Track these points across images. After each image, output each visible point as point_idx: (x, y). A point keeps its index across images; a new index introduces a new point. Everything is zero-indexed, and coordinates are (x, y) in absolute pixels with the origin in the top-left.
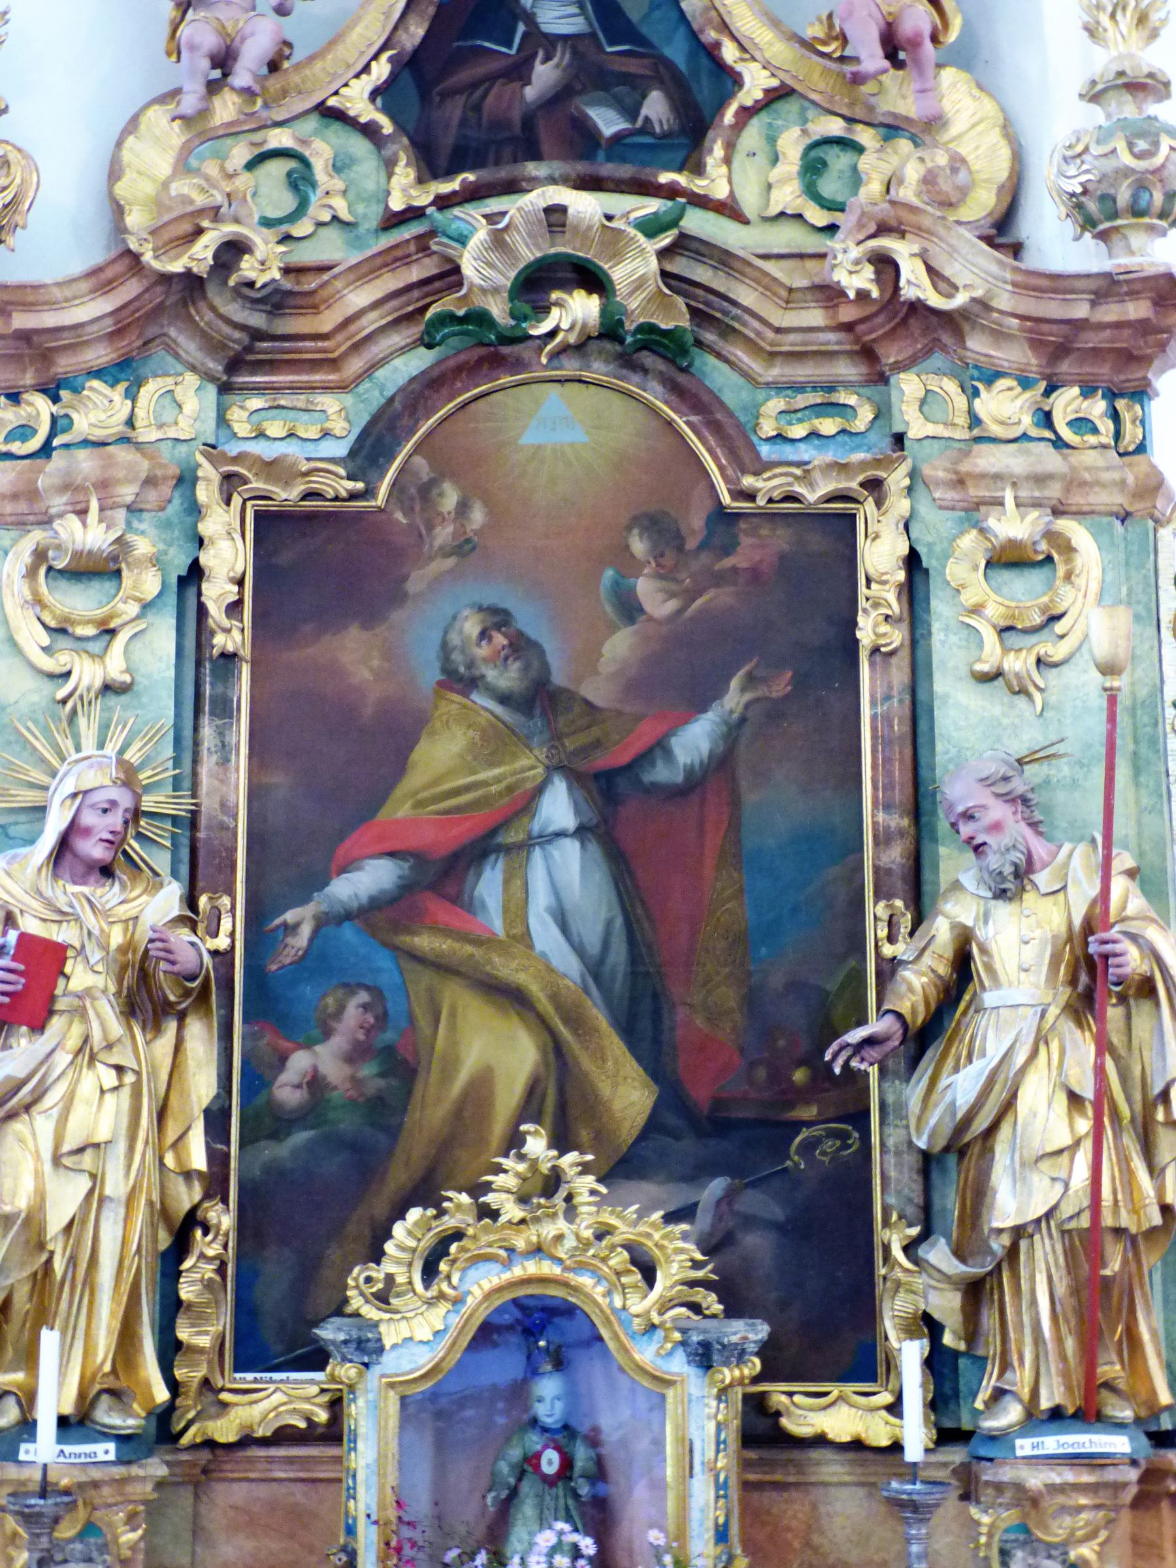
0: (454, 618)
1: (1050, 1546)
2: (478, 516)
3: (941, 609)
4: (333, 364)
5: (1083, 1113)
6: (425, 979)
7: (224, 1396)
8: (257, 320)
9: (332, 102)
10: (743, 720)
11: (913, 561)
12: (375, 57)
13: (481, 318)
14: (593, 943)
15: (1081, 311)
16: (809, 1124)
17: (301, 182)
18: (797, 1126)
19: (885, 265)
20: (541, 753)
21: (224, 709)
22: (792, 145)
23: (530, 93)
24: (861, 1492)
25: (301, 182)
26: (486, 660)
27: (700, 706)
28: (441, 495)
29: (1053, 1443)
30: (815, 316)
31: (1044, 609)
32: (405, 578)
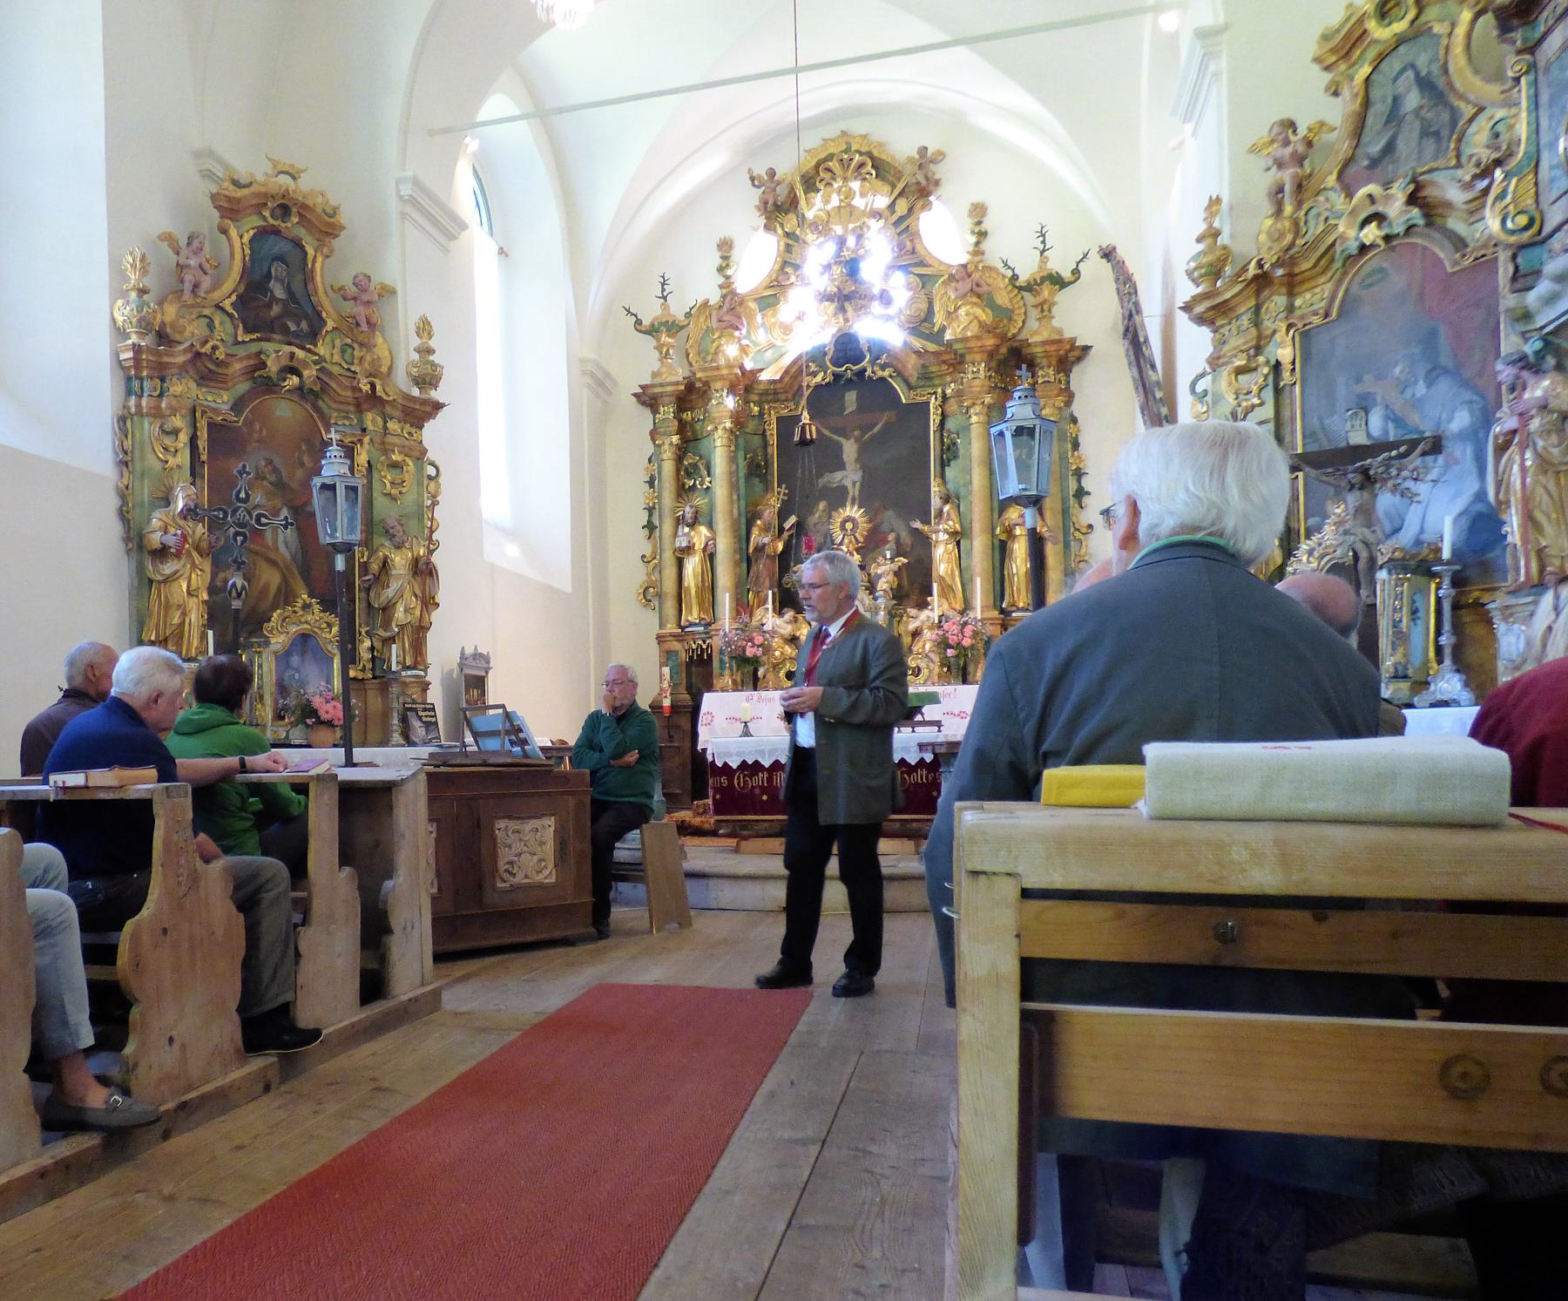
3: (375, 475)
22: (338, 342)
25: (211, 326)
30: (349, 394)
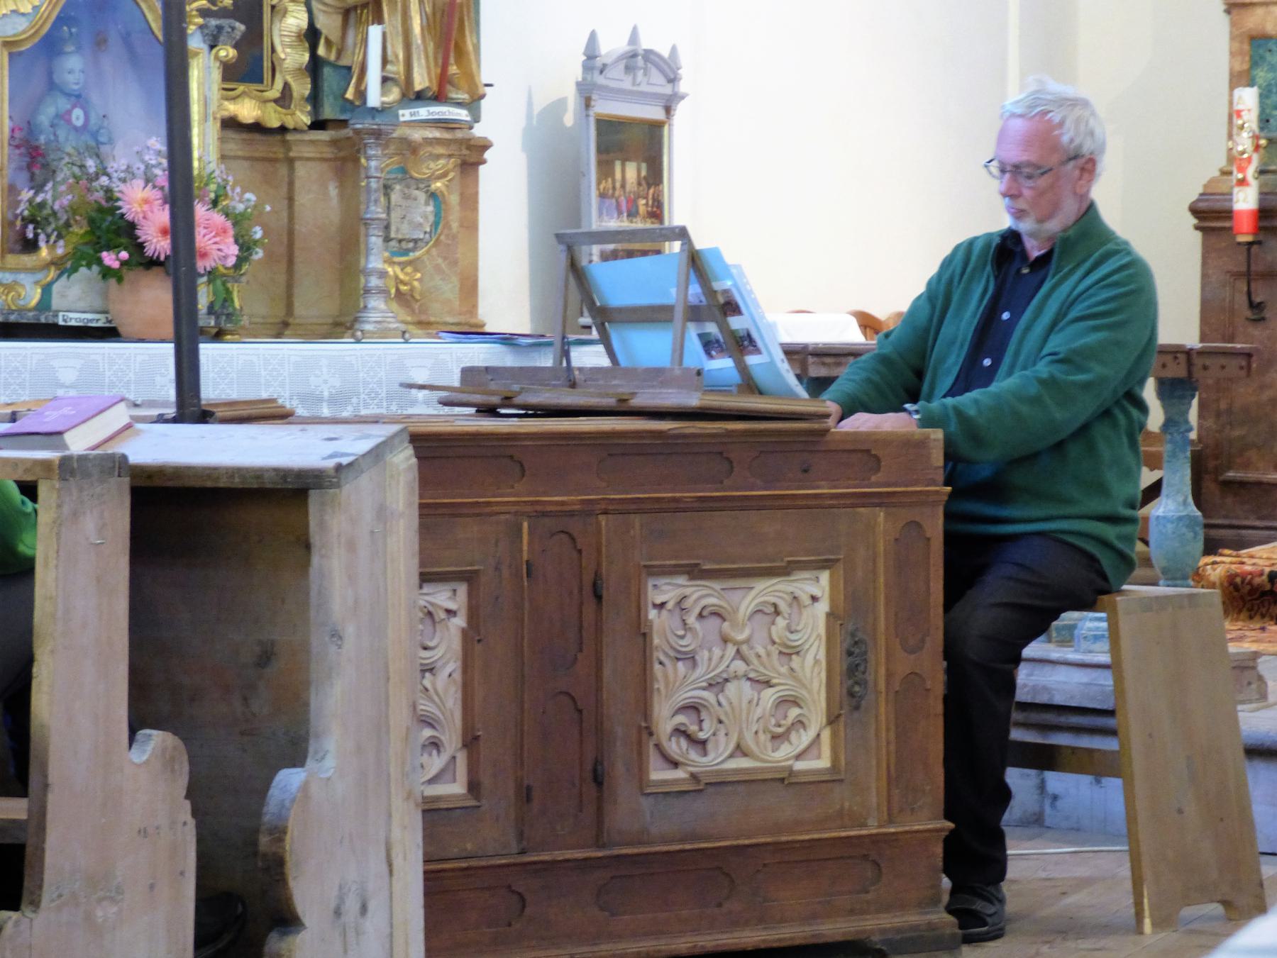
1: (421, 181)
29: (424, 112)
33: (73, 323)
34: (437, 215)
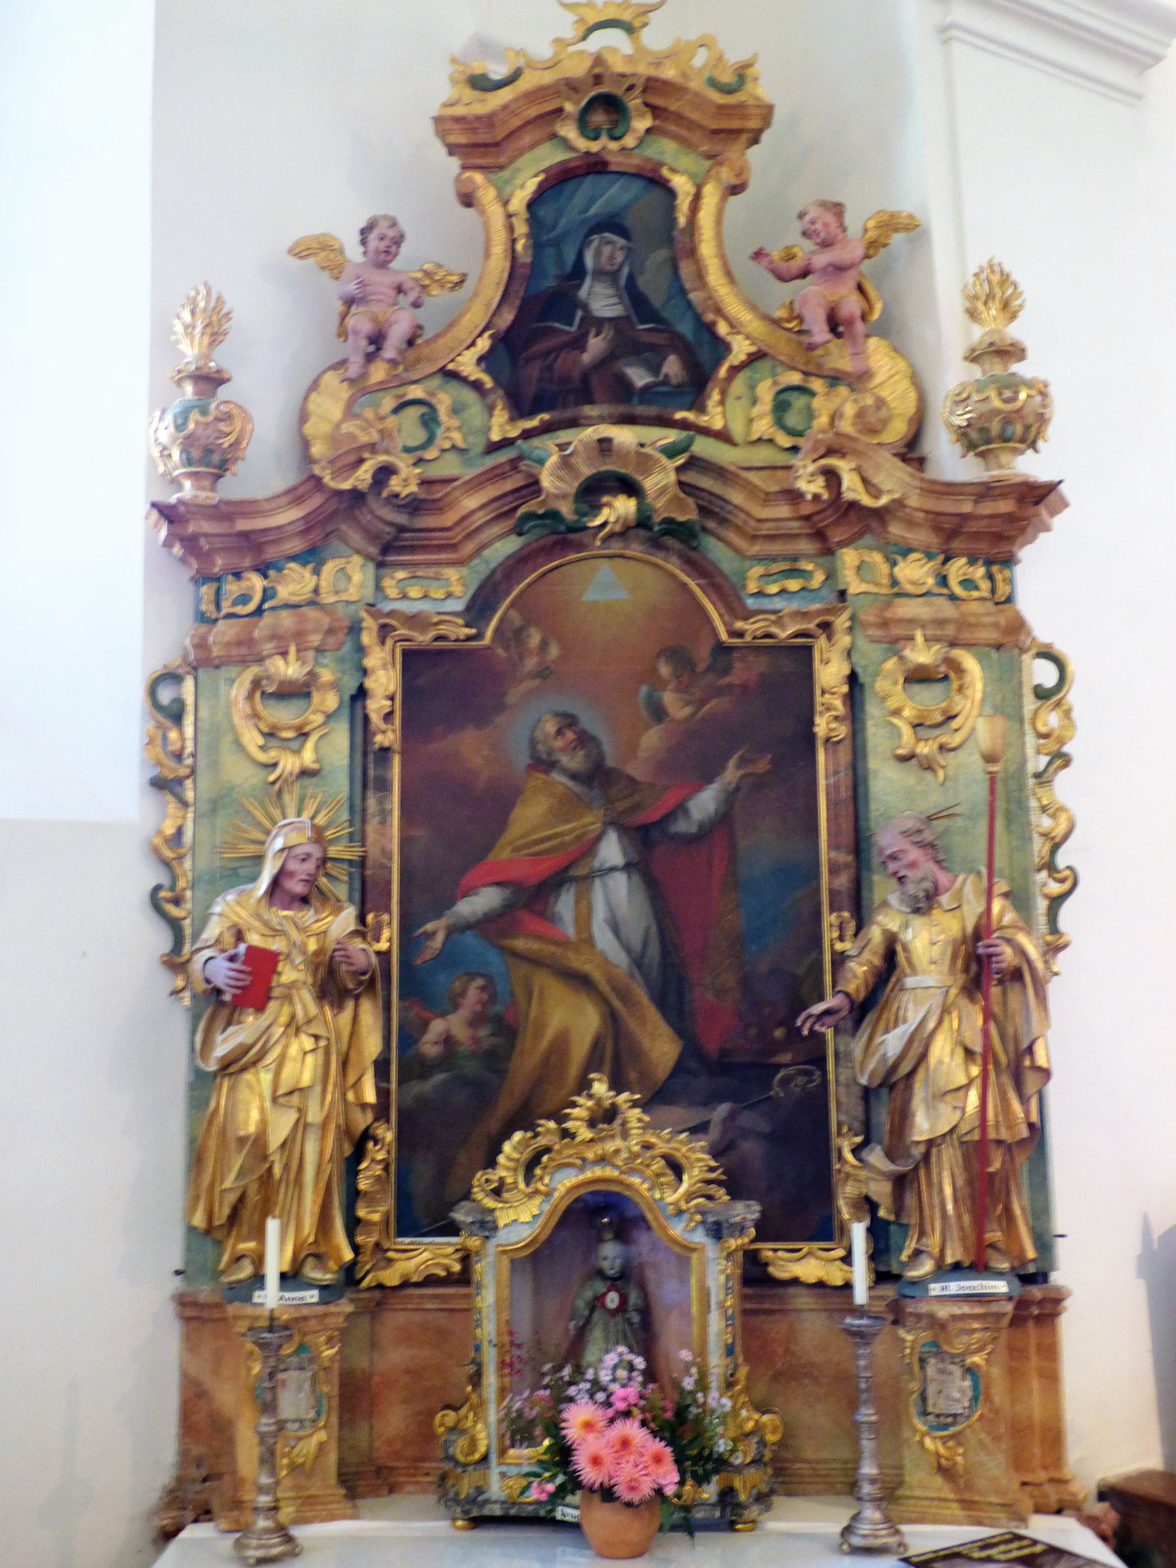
0: (539, 720)
1: (954, 1356)
2: (554, 651)
3: (873, 711)
4: (454, 547)
5: (974, 1061)
6: (523, 969)
7: (390, 1254)
8: (402, 519)
9: (451, 367)
10: (737, 789)
11: (853, 679)
12: (480, 335)
13: (554, 515)
14: (636, 941)
15: (967, 507)
16: (786, 1066)
17: (430, 421)
18: (778, 1067)
19: (832, 477)
20: (600, 813)
21: (383, 785)
22: (766, 392)
23: (586, 358)
24: (823, 1315)
25: (430, 421)
26: (562, 750)
27: (710, 781)
28: (529, 636)
29: (955, 1287)
30: (783, 511)
31: (944, 712)
32: (504, 694)
33: (568, 1519)
34: (975, 1387)
